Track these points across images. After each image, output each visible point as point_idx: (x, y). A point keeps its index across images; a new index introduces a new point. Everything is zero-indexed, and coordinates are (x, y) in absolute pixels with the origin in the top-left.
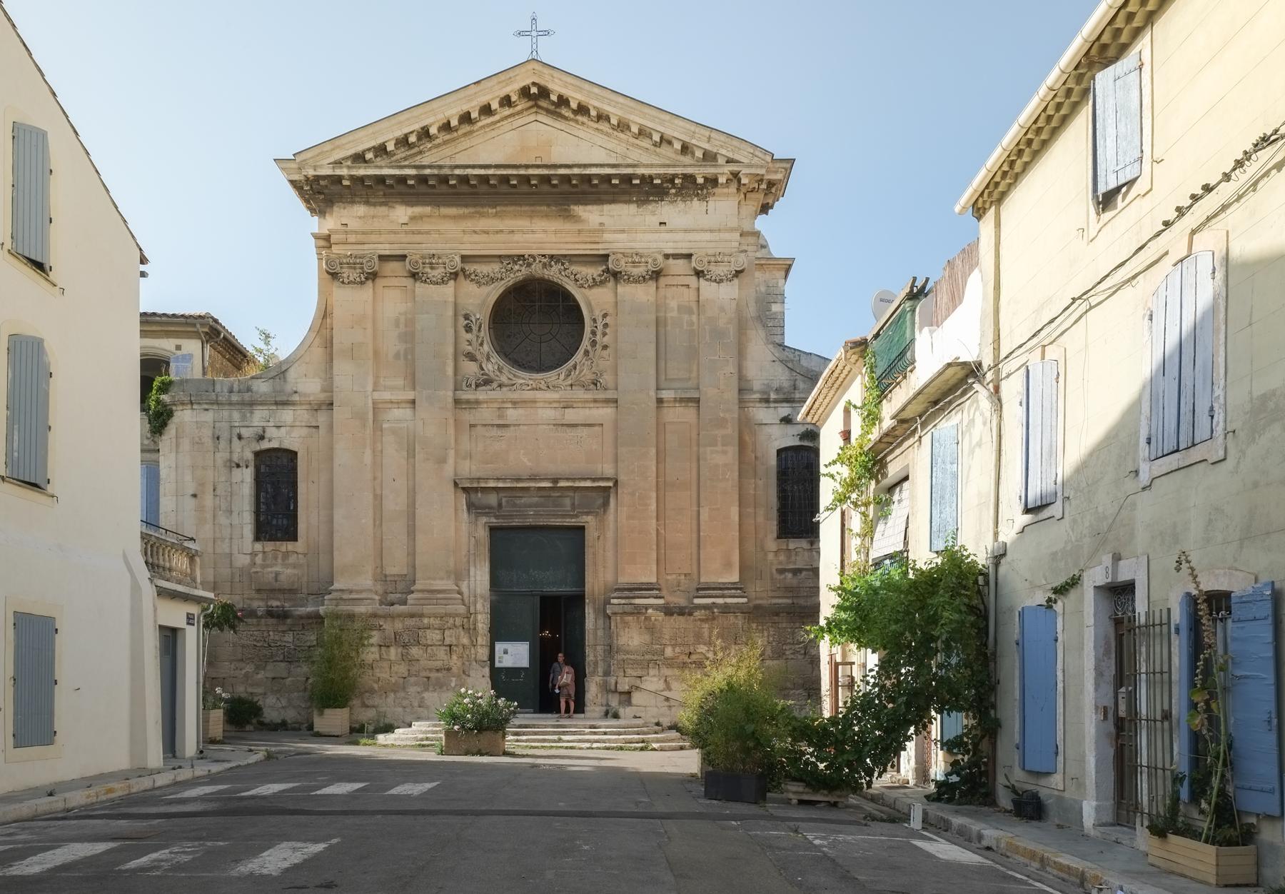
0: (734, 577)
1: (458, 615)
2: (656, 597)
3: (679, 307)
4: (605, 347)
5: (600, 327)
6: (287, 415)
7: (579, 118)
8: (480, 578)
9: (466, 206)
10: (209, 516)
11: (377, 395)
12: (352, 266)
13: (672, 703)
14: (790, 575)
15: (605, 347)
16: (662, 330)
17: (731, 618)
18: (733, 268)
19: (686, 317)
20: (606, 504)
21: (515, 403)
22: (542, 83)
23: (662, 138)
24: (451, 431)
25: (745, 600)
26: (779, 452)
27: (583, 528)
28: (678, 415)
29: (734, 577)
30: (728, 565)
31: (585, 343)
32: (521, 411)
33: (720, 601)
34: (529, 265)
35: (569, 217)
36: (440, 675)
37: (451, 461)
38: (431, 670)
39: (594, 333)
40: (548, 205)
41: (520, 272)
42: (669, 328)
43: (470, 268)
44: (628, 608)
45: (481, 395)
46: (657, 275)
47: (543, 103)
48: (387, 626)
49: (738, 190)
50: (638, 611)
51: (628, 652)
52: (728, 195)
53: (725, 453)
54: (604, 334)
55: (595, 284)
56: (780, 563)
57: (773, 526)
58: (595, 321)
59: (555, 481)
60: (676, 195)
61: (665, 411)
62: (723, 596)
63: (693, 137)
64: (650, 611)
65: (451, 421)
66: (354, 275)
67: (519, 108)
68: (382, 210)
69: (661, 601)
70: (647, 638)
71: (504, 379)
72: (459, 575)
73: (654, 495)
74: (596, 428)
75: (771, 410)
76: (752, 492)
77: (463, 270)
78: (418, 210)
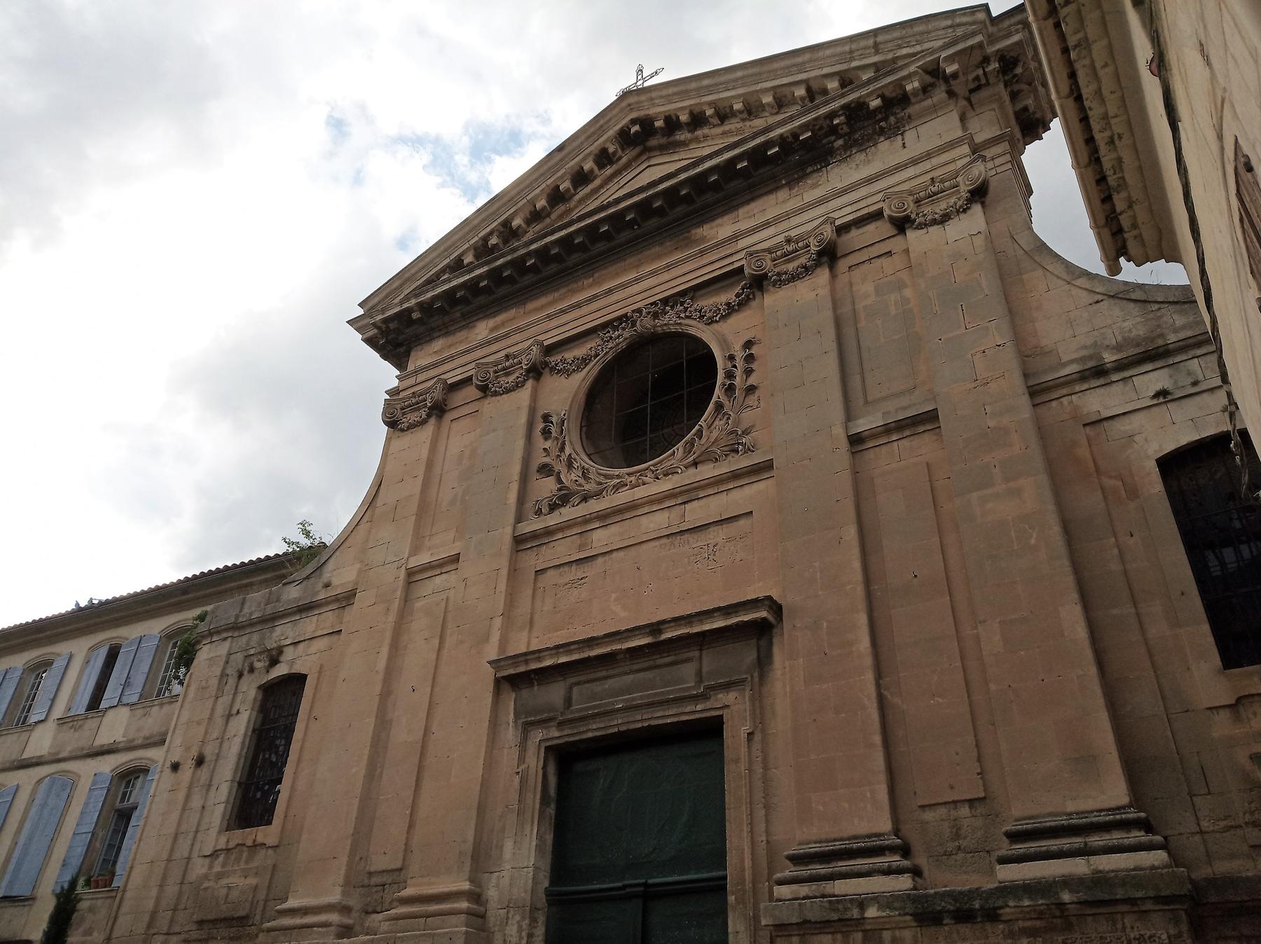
0: (1114, 792)
2: (888, 872)
3: (878, 291)
4: (751, 389)
5: (740, 363)
6: (309, 625)
7: (699, 133)
8: (521, 864)
9: (557, 290)
10: (181, 796)
11: (413, 563)
12: (415, 408)
15: (751, 389)
16: (849, 331)
18: (964, 189)
19: (893, 297)
20: (764, 662)
21: (604, 517)
22: (642, 113)
23: (809, 90)
24: (502, 586)
25: (1159, 857)
26: (1170, 464)
27: (719, 722)
28: (897, 460)
29: (1114, 792)
30: (1084, 763)
31: (718, 391)
33: (1078, 867)
34: (634, 324)
35: (689, 243)
37: (495, 638)
39: (730, 375)
40: (661, 244)
41: (623, 337)
42: (862, 324)
43: (554, 359)
44: (815, 912)
45: (553, 520)
46: (829, 255)
47: (653, 142)
49: (951, 94)
52: (934, 109)
54: (748, 372)
55: (731, 309)
58: (732, 358)
59: (655, 628)
60: (846, 147)
61: (871, 454)
63: (852, 59)
64: (872, 912)
65: (504, 572)
66: (413, 417)
67: (624, 160)
68: (461, 335)
69: (903, 883)
71: (590, 487)
72: (481, 858)
73: (863, 619)
75: (1116, 388)
76: (1115, 567)
77: (546, 364)
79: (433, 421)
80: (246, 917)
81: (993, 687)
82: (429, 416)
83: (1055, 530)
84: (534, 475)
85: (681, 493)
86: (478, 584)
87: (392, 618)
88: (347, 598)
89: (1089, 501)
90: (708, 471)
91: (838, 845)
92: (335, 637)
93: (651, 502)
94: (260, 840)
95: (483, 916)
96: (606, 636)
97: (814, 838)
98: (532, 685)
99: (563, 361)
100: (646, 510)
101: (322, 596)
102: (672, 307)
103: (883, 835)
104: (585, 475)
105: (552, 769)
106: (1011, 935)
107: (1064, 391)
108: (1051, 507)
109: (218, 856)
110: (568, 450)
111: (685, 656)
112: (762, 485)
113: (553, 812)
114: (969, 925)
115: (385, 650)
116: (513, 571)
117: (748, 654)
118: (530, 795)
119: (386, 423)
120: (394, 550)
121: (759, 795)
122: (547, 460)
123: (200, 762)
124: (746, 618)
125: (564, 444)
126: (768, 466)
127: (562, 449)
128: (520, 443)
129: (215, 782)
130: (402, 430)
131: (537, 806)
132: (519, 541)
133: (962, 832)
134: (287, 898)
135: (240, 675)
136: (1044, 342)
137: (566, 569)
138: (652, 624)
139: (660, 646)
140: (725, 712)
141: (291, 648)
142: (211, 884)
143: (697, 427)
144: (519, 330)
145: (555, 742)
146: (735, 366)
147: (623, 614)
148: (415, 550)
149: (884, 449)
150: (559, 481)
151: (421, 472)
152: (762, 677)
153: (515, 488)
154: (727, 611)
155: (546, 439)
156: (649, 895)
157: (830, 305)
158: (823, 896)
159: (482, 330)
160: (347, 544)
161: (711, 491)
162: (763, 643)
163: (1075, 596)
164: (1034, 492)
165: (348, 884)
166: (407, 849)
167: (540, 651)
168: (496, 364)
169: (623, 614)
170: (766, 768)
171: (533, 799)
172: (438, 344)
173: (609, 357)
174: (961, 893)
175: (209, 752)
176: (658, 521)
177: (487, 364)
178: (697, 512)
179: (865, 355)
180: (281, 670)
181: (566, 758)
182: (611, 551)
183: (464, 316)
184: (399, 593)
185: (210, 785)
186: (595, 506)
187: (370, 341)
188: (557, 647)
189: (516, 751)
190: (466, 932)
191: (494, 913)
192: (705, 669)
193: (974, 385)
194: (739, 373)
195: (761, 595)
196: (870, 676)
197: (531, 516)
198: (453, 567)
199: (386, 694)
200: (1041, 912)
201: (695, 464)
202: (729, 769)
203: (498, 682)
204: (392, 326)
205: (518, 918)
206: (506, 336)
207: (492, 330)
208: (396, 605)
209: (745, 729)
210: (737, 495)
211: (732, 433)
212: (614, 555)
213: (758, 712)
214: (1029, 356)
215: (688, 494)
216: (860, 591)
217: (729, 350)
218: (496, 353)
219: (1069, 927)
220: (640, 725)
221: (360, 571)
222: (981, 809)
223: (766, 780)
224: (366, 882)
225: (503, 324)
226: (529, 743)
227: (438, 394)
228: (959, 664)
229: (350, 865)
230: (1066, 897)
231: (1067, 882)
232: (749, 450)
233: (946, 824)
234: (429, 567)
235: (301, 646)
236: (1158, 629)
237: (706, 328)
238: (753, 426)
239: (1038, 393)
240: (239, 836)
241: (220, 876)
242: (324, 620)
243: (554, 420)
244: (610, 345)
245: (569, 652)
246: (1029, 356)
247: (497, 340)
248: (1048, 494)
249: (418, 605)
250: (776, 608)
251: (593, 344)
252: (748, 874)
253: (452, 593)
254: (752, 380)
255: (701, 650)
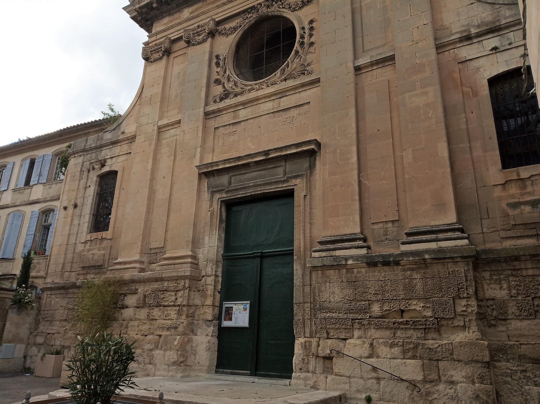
0: (451, 218)
1: (184, 278)
2: (357, 247)
5: (307, 31)
6: (117, 150)
8: (212, 245)
10: (69, 220)
11: (160, 123)
12: (157, 51)
13: (381, 374)
14: (527, 209)
15: (312, 44)
16: (358, 17)
17: (451, 267)
20: (312, 167)
24: (200, 134)
25: (466, 241)
26: (493, 82)
29: (451, 218)
32: (249, 109)
33: (433, 246)
34: (258, 11)
36: (168, 333)
38: (163, 328)
39: (302, 37)
41: (253, 17)
42: (364, 13)
43: (220, 28)
44: (327, 262)
45: (222, 105)
48: (141, 289)
50: (338, 265)
51: (330, 310)
53: (426, 93)
54: (311, 35)
56: (513, 196)
57: (495, 155)
58: (303, 28)
59: (267, 153)
61: (364, 76)
62: (437, 240)
64: (350, 262)
65: (201, 128)
66: (156, 56)
68: (176, 15)
69: (364, 251)
70: (349, 291)
71: (238, 90)
72: (196, 243)
73: (354, 149)
74: (305, 107)
75: (475, 46)
76: (464, 126)
78: (194, 7)
79: (165, 58)
80: (102, 265)
81: (406, 176)
82: (163, 55)
83: (440, 110)
84: (212, 84)
85: (279, 93)
86: (190, 132)
87: (153, 147)
88: (132, 139)
89: (456, 97)
90: (291, 83)
91: (338, 238)
92: (129, 155)
93: (265, 97)
94: (104, 236)
95: (197, 264)
96: (245, 156)
97: (329, 235)
98: (214, 176)
99: (225, 29)
100: (263, 101)
101: (121, 137)
102: (276, 3)
103: (356, 234)
104: (236, 85)
105: (223, 209)
106: (404, 270)
107: (452, 47)
108: (440, 100)
109: (87, 243)
110: (228, 73)
111: (279, 164)
112: (315, 90)
113: (224, 226)
114: (388, 267)
115: (151, 161)
116: (205, 127)
117: (305, 163)
118: (215, 219)
119: (144, 59)
120: (151, 117)
121: (307, 219)
122: (218, 77)
123: (76, 206)
124: (305, 148)
125: (226, 69)
126: (318, 81)
127: (225, 72)
128: (206, 69)
129: (83, 214)
130: (151, 62)
131: (218, 223)
132: (207, 114)
133: (388, 233)
134: (117, 259)
135: (89, 171)
136: (446, 23)
137: (228, 127)
138: (265, 151)
139: (268, 160)
140: (295, 187)
141: (110, 159)
142: (86, 253)
143: (287, 62)
144: (204, 13)
145: (225, 199)
146: (305, 33)
147: (253, 147)
148: (161, 118)
149: (370, 73)
150: (224, 87)
151: (161, 82)
152: (311, 173)
153: (204, 89)
154: (297, 145)
155: (217, 67)
156: (263, 256)
157: (350, 3)
158: (331, 256)
159: (186, 13)
160: (129, 115)
161: (292, 92)
162: (312, 159)
163: (445, 139)
164: (433, 93)
165: (142, 253)
166: (165, 240)
167: (217, 162)
168: (193, 30)
169: (253, 147)
170: (311, 209)
171: (216, 221)
172: (166, 20)
173: (246, 27)
174: (386, 255)
175: (79, 202)
176: (268, 106)
177: (189, 30)
178: (285, 102)
179: (364, 28)
180: (106, 169)
181: (230, 206)
182: (248, 119)
183: (177, 6)
184: (155, 137)
185: (81, 216)
186: (240, 99)
187: (133, 18)
188: (225, 160)
189: (208, 203)
190: (191, 270)
191: (202, 263)
192: (287, 170)
193: (412, 43)
194: (306, 36)
195: (312, 138)
196: (356, 172)
197: (212, 103)
198: (178, 125)
199: (152, 179)
200: (416, 262)
201: (285, 80)
202: (296, 209)
203: (200, 175)
204: (144, 10)
205: (211, 265)
206: (198, 16)
207: (191, 13)
208: (154, 142)
209: (304, 194)
210: (303, 94)
211: (302, 65)
212: (249, 121)
213: (309, 187)
214: (437, 29)
215: (282, 94)
216: (354, 137)
217: (302, 24)
218: (193, 24)
219: (426, 267)
220: (260, 192)
221: (137, 127)
222: (396, 224)
223: (311, 213)
224: (149, 252)
225: (196, 10)
226: (214, 199)
227: (167, 45)
228: (393, 167)
229: (142, 246)
230: (427, 257)
231: (427, 251)
232: (310, 73)
233: (382, 230)
234: (168, 125)
235: (114, 159)
236: (478, 153)
237: (291, 13)
238: (312, 62)
239: (440, 47)
240: (94, 235)
241: (89, 250)
242: (124, 148)
243: (221, 58)
244: (247, 21)
245: (230, 163)
246: (437, 29)
247: (193, 18)
248: (439, 93)
249: (164, 142)
250: (319, 145)
251: (239, 21)
252: (302, 249)
253: (178, 137)
254: (312, 40)
255: (286, 162)
